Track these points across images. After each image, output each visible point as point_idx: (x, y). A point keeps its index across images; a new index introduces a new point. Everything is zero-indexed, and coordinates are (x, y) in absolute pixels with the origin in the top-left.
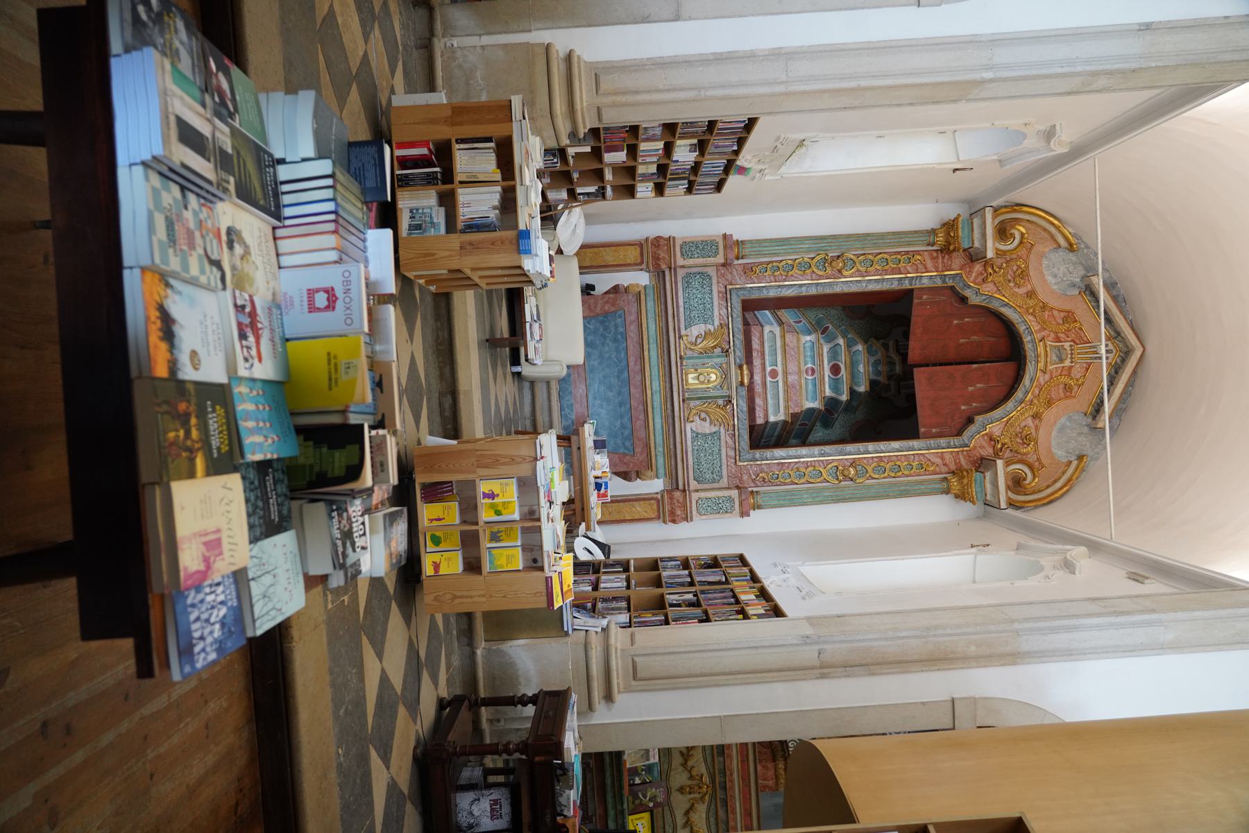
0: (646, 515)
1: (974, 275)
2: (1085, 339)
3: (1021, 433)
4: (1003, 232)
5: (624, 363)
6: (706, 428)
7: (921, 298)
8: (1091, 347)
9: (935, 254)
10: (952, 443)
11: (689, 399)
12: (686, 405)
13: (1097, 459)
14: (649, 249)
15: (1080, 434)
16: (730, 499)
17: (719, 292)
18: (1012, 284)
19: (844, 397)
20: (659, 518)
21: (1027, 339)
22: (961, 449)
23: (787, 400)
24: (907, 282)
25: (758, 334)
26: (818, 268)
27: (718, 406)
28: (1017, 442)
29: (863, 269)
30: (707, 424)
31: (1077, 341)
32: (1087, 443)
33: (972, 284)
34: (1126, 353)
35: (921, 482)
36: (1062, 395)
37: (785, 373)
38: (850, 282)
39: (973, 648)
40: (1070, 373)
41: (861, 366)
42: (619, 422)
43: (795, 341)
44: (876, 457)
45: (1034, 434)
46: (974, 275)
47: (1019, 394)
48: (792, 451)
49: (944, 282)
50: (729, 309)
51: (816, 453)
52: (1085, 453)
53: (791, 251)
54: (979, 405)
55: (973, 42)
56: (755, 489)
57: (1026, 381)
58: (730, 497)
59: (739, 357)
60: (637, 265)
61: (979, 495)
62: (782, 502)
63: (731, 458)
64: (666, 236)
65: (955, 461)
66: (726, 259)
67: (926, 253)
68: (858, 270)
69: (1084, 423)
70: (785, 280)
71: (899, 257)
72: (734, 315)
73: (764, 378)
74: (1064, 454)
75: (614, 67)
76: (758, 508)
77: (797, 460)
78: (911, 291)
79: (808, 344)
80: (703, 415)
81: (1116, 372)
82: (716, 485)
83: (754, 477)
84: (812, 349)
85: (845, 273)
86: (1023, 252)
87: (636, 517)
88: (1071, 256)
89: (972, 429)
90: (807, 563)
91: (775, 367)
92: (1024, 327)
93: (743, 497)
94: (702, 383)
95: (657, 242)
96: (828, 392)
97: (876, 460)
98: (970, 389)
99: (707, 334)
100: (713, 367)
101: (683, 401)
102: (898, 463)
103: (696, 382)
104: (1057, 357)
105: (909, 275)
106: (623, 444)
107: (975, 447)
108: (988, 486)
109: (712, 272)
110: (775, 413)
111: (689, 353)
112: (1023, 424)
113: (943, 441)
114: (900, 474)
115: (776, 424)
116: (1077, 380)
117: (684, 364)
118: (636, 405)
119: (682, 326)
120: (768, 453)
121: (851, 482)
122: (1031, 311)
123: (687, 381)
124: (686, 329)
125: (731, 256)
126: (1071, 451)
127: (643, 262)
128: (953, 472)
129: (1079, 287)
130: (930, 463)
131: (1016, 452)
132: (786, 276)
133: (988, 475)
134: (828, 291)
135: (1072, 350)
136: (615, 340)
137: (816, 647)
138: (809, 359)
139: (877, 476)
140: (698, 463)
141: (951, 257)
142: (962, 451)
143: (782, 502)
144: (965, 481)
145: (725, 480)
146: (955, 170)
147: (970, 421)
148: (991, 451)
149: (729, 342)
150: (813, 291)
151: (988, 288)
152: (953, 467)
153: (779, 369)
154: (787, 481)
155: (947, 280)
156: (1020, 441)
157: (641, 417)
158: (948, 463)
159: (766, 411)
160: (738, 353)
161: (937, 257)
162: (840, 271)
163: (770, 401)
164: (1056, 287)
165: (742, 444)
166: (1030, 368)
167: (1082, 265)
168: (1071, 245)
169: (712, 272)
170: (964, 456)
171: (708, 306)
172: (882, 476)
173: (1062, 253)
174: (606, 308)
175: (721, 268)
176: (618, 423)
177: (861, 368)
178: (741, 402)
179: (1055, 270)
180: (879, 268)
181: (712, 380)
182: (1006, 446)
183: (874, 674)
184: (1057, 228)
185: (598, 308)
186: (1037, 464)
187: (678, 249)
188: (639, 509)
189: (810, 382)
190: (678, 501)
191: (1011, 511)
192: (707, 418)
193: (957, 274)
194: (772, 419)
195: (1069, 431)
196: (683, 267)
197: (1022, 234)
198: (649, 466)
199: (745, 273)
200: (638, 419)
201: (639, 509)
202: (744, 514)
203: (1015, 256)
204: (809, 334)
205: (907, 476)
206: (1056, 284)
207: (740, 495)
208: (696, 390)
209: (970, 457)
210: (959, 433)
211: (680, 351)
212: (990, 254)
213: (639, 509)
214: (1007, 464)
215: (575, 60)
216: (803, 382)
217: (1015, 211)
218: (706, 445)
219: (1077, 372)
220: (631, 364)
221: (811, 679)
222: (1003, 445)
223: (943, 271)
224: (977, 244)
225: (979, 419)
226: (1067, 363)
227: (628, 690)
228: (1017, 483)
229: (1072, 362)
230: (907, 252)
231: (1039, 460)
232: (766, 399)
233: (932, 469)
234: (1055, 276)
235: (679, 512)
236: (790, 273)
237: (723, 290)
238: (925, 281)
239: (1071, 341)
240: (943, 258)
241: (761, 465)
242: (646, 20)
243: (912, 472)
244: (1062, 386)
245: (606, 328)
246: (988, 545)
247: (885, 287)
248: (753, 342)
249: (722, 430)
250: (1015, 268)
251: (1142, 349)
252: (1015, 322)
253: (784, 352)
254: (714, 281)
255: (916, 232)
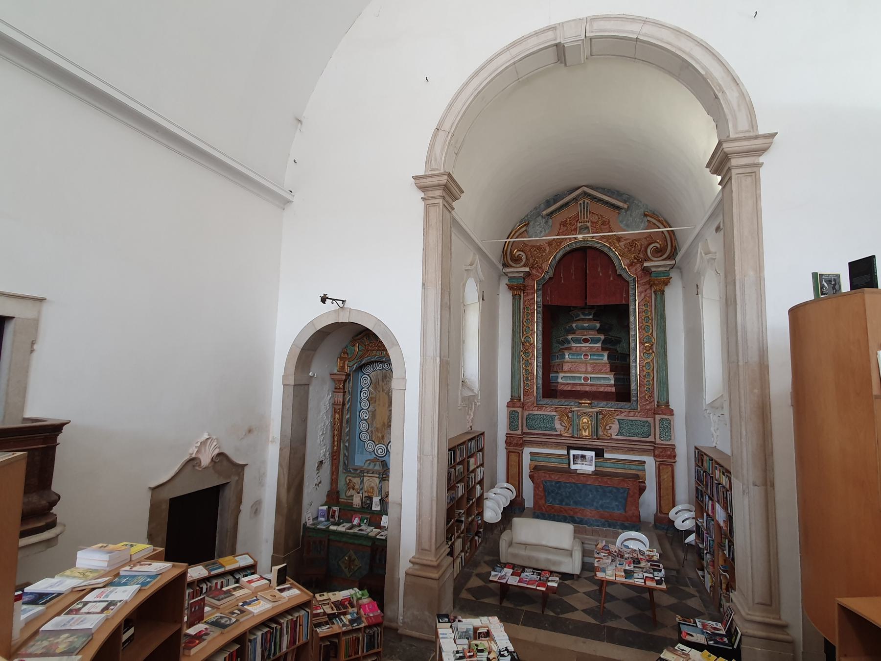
0: (670, 473)
1: (537, 274)
2: (576, 215)
3: (628, 248)
4: (517, 260)
5: (573, 485)
6: (615, 427)
7: (548, 300)
8: (581, 212)
9: (526, 294)
10: (633, 287)
11: (597, 436)
12: (601, 437)
13: (647, 205)
14: (511, 448)
15: (631, 215)
16: (661, 420)
17: (537, 410)
18: (544, 254)
19: (602, 337)
20: (672, 467)
21: (574, 246)
22: (636, 282)
23: (600, 372)
24: (539, 309)
25: (563, 386)
26: (528, 356)
27: (603, 419)
28: (634, 250)
29: (531, 332)
30: (613, 426)
31: (577, 219)
32: (637, 211)
33: (543, 275)
34: (586, 194)
35: (656, 306)
36: (607, 226)
37: (586, 372)
38: (536, 339)
39: (756, 391)
40: (594, 222)
41: (585, 325)
42: (608, 494)
43: (568, 364)
44: (639, 330)
45: (628, 241)
46: (537, 274)
47: (605, 250)
48: (632, 378)
49: (540, 290)
50: (547, 406)
51: (634, 364)
52: (643, 212)
53: (518, 372)
54: (611, 270)
55: (423, 365)
56: (656, 403)
57: (598, 246)
58: (660, 420)
59: (574, 404)
60: (519, 455)
61: (666, 275)
62: (665, 389)
63: (635, 414)
64: (506, 438)
65: (644, 285)
66: (520, 407)
67: (524, 299)
68: (531, 335)
69: (625, 214)
70: (534, 374)
71: (525, 313)
72: (551, 404)
73: (587, 385)
74: (643, 224)
75: (419, 540)
76: (668, 403)
77: (638, 376)
78: (543, 305)
79: (570, 357)
80: (608, 427)
81: (596, 198)
82: (652, 425)
83: (648, 402)
84: (573, 355)
85: (532, 343)
86: (527, 249)
87: (671, 479)
88: (531, 224)
89: (624, 275)
90: (705, 397)
91: (582, 378)
92: (568, 247)
93: (661, 412)
94: (588, 427)
95: (508, 443)
96: (599, 345)
97: (640, 330)
98: (601, 274)
99: (560, 420)
100: (579, 421)
101: (598, 439)
102: (643, 318)
103: (587, 430)
104: (585, 230)
105: (535, 308)
106: (622, 493)
107: (636, 274)
108: (660, 269)
109: (526, 413)
110: (607, 380)
111: (571, 431)
112: (623, 247)
113: (631, 292)
114: (650, 318)
115: (616, 379)
116: (599, 219)
117: (576, 436)
118: (598, 482)
119: (555, 433)
120: (633, 392)
121: (654, 346)
122: (559, 244)
123: (586, 436)
124: (557, 431)
125: (518, 404)
126: (641, 221)
127: (518, 452)
128: (651, 286)
129: (548, 219)
130: (644, 300)
131: (640, 251)
132: (531, 373)
133: (653, 269)
134: (541, 351)
135: (582, 222)
136: (559, 488)
137: (751, 486)
138: (578, 357)
139: (651, 331)
140: (637, 434)
141: (528, 286)
142: (638, 281)
143: (665, 389)
144: (656, 282)
145: (649, 419)
146: (483, 299)
147: (620, 275)
148: (639, 265)
149: (566, 408)
150: (541, 359)
151: (545, 267)
152: (648, 286)
153: (583, 376)
154: (651, 383)
155: (539, 288)
156: (633, 249)
157: (606, 481)
158: (643, 289)
159: (608, 385)
160: (572, 404)
161: (527, 293)
162: (531, 345)
163: (602, 382)
164: (547, 232)
165: (626, 407)
166: (590, 244)
167: (536, 218)
168: (525, 225)
169: (526, 413)
170: (640, 280)
171: (545, 417)
172: (651, 327)
173: (530, 229)
174: (541, 489)
175: (524, 408)
176: (608, 494)
177: (586, 325)
178: (601, 405)
179: (538, 232)
180: (530, 324)
181: (587, 421)
182: (636, 257)
183: (772, 453)
184: (516, 232)
185: (540, 493)
186: (648, 239)
187: (512, 432)
188: (665, 476)
189: (592, 357)
190: (661, 452)
191: (678, 258)
192: (610, 425)
193: (537, 282)
194: (612, 382)
195: (629, 222)
196: (522, 430)
197: (518, 251)
198: (637, 476)
199: (528, 395)
200: (606, 482)
201: (665, 476)
202: (671, 413)
203: (529, 253)
204: (565, 355)
205: (652, 313)
206: (545, 231)
207: (659, 414)
208: (592, 432)
209: (642, 277)
210: (628, 282)
211: (569, 437)
212: (527, 269)
213: (666, 476)
214: (647, 259)
215: (414, 560)
216: (592, 361)
217: (506, 254)
218: (626, 428)
219: (595, 219)
220: (574, 481)
221: (774, 494)
222: (635, 258)
223: (535, 290)
224: (522, 275)
225: (619, 272)
226: (589, 224)
227: (778, 611)
228: (659, 252)
229: (589, 222)
230: (524, 308)
231: (646, 238)
232: (601, 385)
233: (648, 299)
234: (541, 232)
235: (669, 453)
236: (530, 371)
237: (536, 408)
238: (539, 300)
239: (577, 223)
240: (527, 290)
241: (640, 398)
242: (400, 519)
243: (649, 310)
244: (602, 227)
245: (553, 492)
246: (697, 286)
247: (541, 320)
248: (567, 389)
249: (617, 417)
250: (535, 253)
251: (584, 187)
252: (564, 252)
253: (574, 372)
254: (531, 412)
255: (513, 305)
